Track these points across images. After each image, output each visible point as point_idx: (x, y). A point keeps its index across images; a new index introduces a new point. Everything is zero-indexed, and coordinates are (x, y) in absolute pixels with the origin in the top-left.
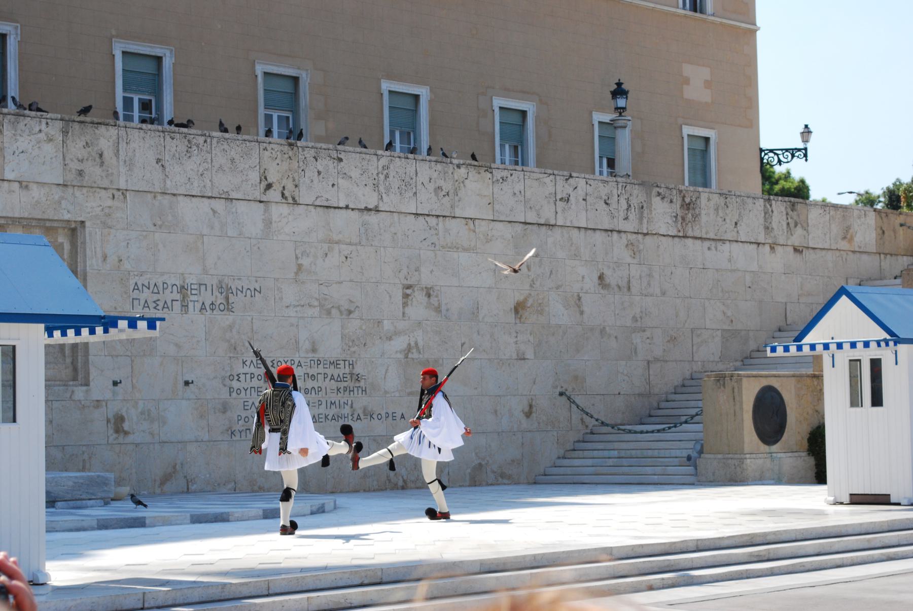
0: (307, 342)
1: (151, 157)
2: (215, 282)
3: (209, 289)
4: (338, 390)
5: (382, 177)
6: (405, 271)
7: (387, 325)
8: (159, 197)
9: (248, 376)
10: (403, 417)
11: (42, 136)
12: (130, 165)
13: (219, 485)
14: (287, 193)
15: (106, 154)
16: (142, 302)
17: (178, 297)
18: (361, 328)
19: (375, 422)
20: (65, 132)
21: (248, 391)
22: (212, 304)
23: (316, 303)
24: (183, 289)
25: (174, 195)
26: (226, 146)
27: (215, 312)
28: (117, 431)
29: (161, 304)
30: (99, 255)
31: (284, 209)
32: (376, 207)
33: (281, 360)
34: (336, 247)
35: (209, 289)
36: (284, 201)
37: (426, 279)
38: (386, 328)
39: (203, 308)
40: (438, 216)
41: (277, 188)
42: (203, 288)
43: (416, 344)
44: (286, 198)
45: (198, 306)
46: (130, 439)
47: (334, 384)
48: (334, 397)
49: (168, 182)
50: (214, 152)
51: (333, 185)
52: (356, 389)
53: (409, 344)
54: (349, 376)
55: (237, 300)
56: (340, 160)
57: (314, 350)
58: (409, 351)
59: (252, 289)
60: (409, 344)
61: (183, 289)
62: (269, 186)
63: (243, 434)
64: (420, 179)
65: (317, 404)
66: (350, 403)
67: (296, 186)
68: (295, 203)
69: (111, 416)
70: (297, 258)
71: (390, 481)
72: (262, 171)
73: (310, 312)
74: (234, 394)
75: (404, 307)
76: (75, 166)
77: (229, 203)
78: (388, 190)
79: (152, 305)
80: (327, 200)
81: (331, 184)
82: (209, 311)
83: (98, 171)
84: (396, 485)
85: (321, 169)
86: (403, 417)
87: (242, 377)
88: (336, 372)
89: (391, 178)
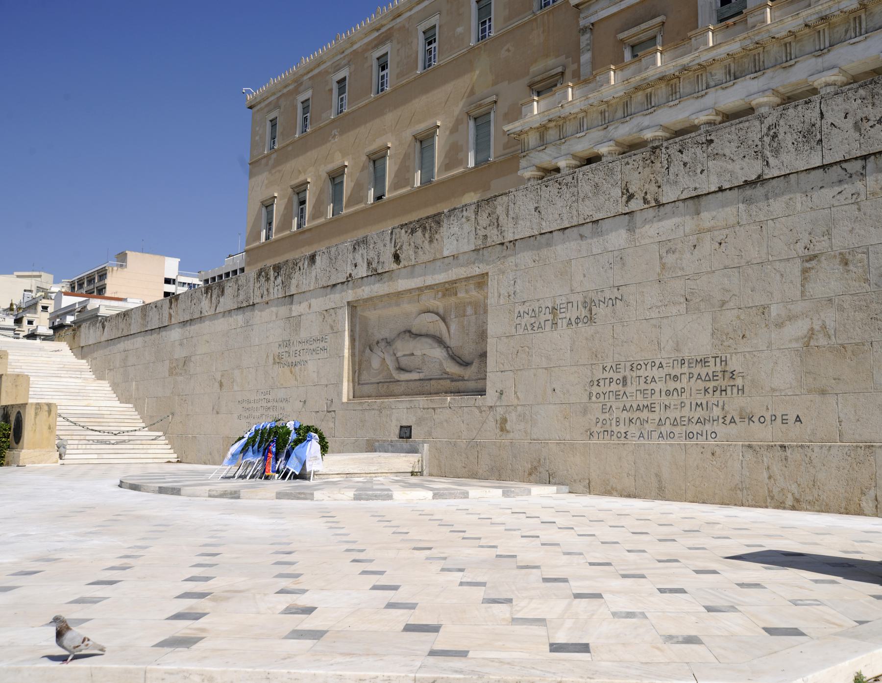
0: (670, 342)
1: (532, 208)
2: (580, 298)
3: (575, 305)
4: (706, 390)
5: (767, 140)
6: (805, 239)
7: (774, 310)
8: (538, 237)
9: (607, 381)
10: (798, 419)
11: (464, 220)
12: (516, 219)
13: (575, 481)
14: (648, 197)
15: (501, 218)
16: (523, 325)
17: (550, 317)
18: (738, 317)
19: (755, 426)
20: (476, 213)
21: (607, 395)
22: (578, 318)
23: (683, 300)
24: (554, 310)
25: (551, 232)
26: (591, 175)
27: (580, 325)
28: (502, 430)
29: (536, 325)
30: (496, 294)
31: (651, 213)
32: (759, 177)
33: (641, 363)
34: (708, 236)
35: (575, 305)
36: (646, 206)
37: (842, 240)
38: (774, 314)
39: (570, 323)
40: (865, 158)
41: (639, 196)
42: (570, 305)
43: (824, 327)
44: (648, 203)
45: (565, 322)
46: (511, 435)
47: (701, 385)
48: (701, 399)
49: (544, 223)
50: (580, 184)
51: (702, 171)
52: (729, 389)
53: (812, 329)
54: (720, 375)
55: (601, 311)
56: (711, 141)
57: (678, 350)
58: (810, 338)
59: (613, 298)
60: (812, 329)
61: (554, 310)
62: (631, 197)
63: (601, 435)
64: (829, 118)
65: (679, 407)
66: (721, 404)
67: (659, 187)
68: (659, 205)
69: (498, 418)
70: (661, 258)
71: (772, 498)
72: (624, 185)
73: (674, 310)
74: (594, 398)
75: (803, 286)
76: (481, 233)
77: (595, 226)
78: (776, 152)
79: (529, 328)
80: (696, 189)
81: (699, 171)
82: (574, 325)
83: (495, 231)
84: (783, 502)
85: (686, 159)
86: (798, 419)
87: (602, 383)
88: (703, 372)
89: (780, 137)
